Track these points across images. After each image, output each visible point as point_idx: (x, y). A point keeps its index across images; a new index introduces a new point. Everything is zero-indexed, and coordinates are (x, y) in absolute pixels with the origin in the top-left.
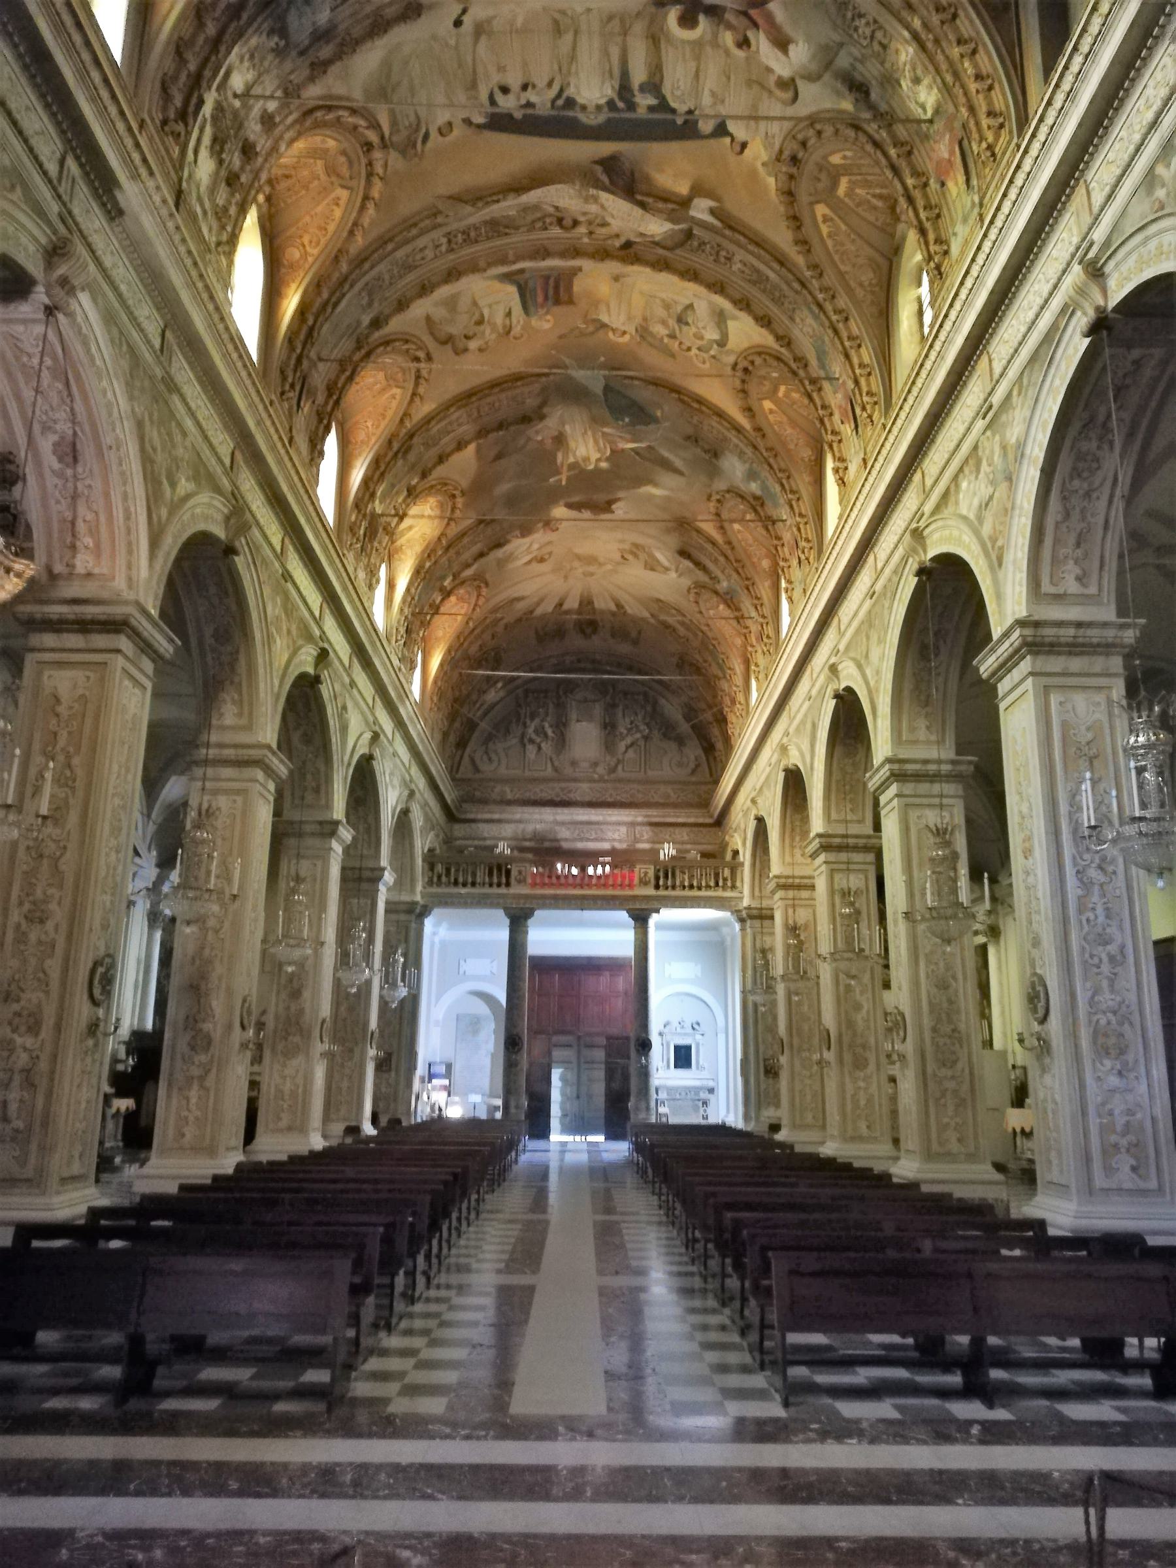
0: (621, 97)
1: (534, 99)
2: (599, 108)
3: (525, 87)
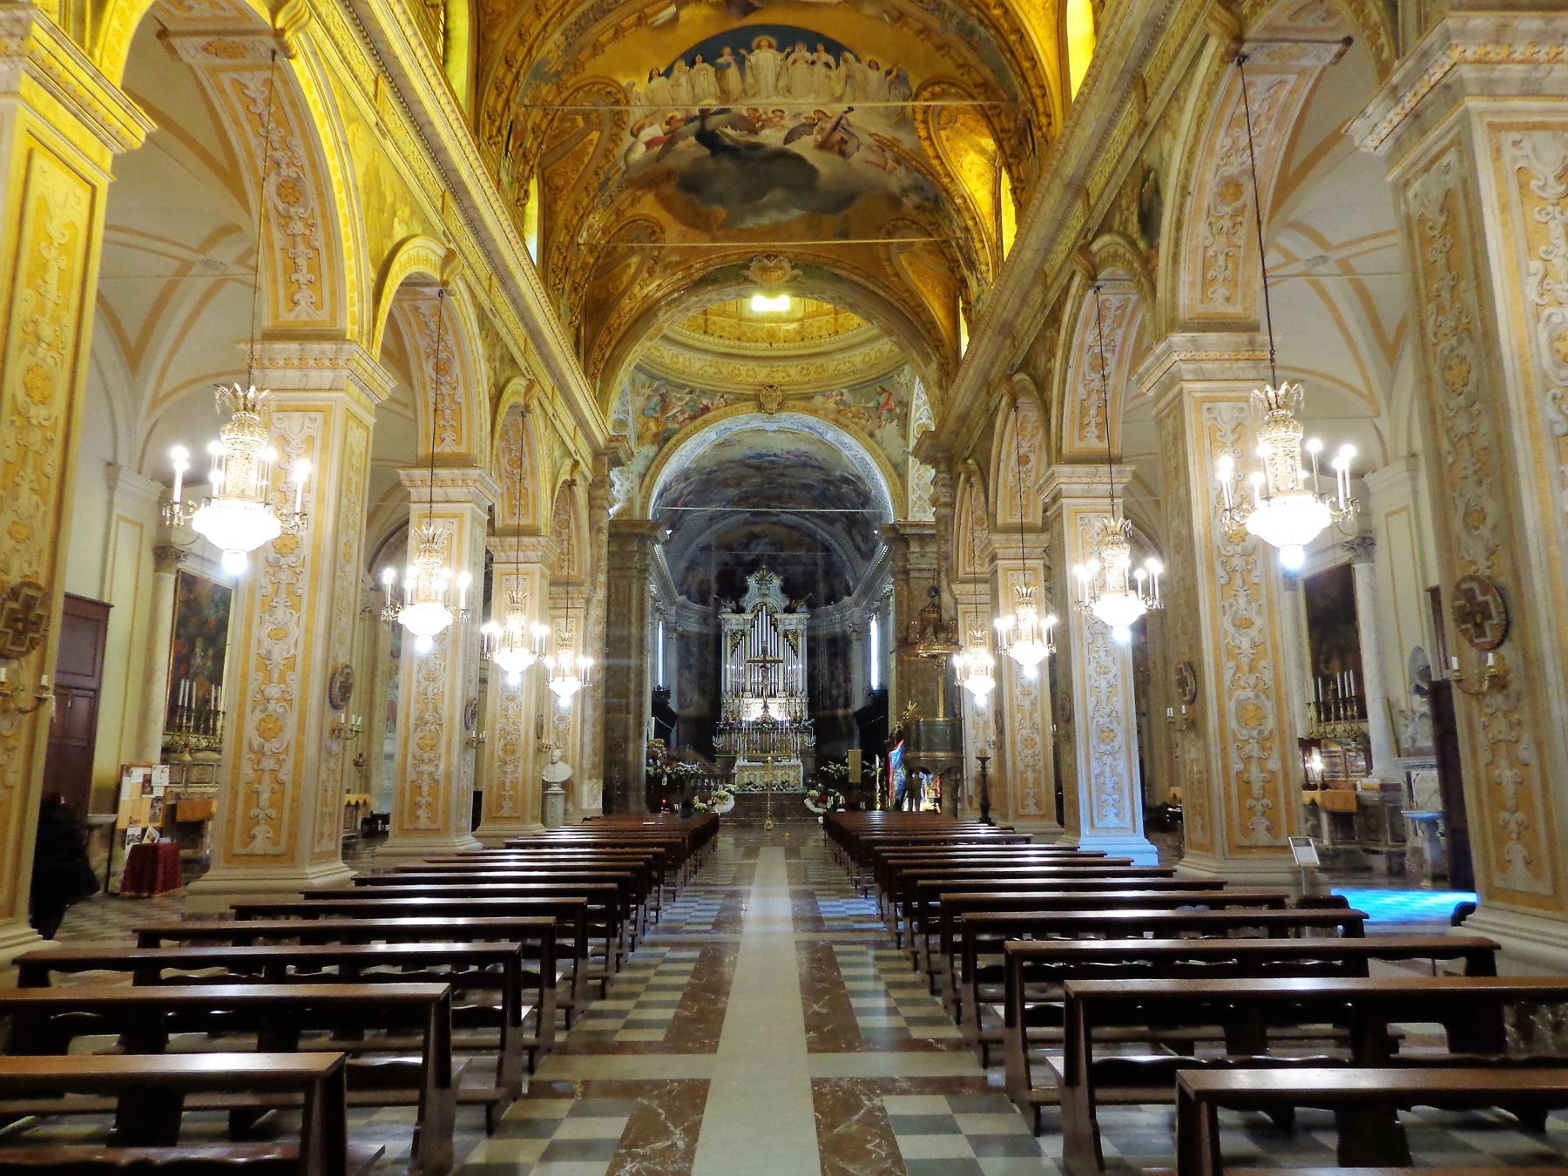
1: (808, 55)
2: (759, 47)
3: (813, 63)
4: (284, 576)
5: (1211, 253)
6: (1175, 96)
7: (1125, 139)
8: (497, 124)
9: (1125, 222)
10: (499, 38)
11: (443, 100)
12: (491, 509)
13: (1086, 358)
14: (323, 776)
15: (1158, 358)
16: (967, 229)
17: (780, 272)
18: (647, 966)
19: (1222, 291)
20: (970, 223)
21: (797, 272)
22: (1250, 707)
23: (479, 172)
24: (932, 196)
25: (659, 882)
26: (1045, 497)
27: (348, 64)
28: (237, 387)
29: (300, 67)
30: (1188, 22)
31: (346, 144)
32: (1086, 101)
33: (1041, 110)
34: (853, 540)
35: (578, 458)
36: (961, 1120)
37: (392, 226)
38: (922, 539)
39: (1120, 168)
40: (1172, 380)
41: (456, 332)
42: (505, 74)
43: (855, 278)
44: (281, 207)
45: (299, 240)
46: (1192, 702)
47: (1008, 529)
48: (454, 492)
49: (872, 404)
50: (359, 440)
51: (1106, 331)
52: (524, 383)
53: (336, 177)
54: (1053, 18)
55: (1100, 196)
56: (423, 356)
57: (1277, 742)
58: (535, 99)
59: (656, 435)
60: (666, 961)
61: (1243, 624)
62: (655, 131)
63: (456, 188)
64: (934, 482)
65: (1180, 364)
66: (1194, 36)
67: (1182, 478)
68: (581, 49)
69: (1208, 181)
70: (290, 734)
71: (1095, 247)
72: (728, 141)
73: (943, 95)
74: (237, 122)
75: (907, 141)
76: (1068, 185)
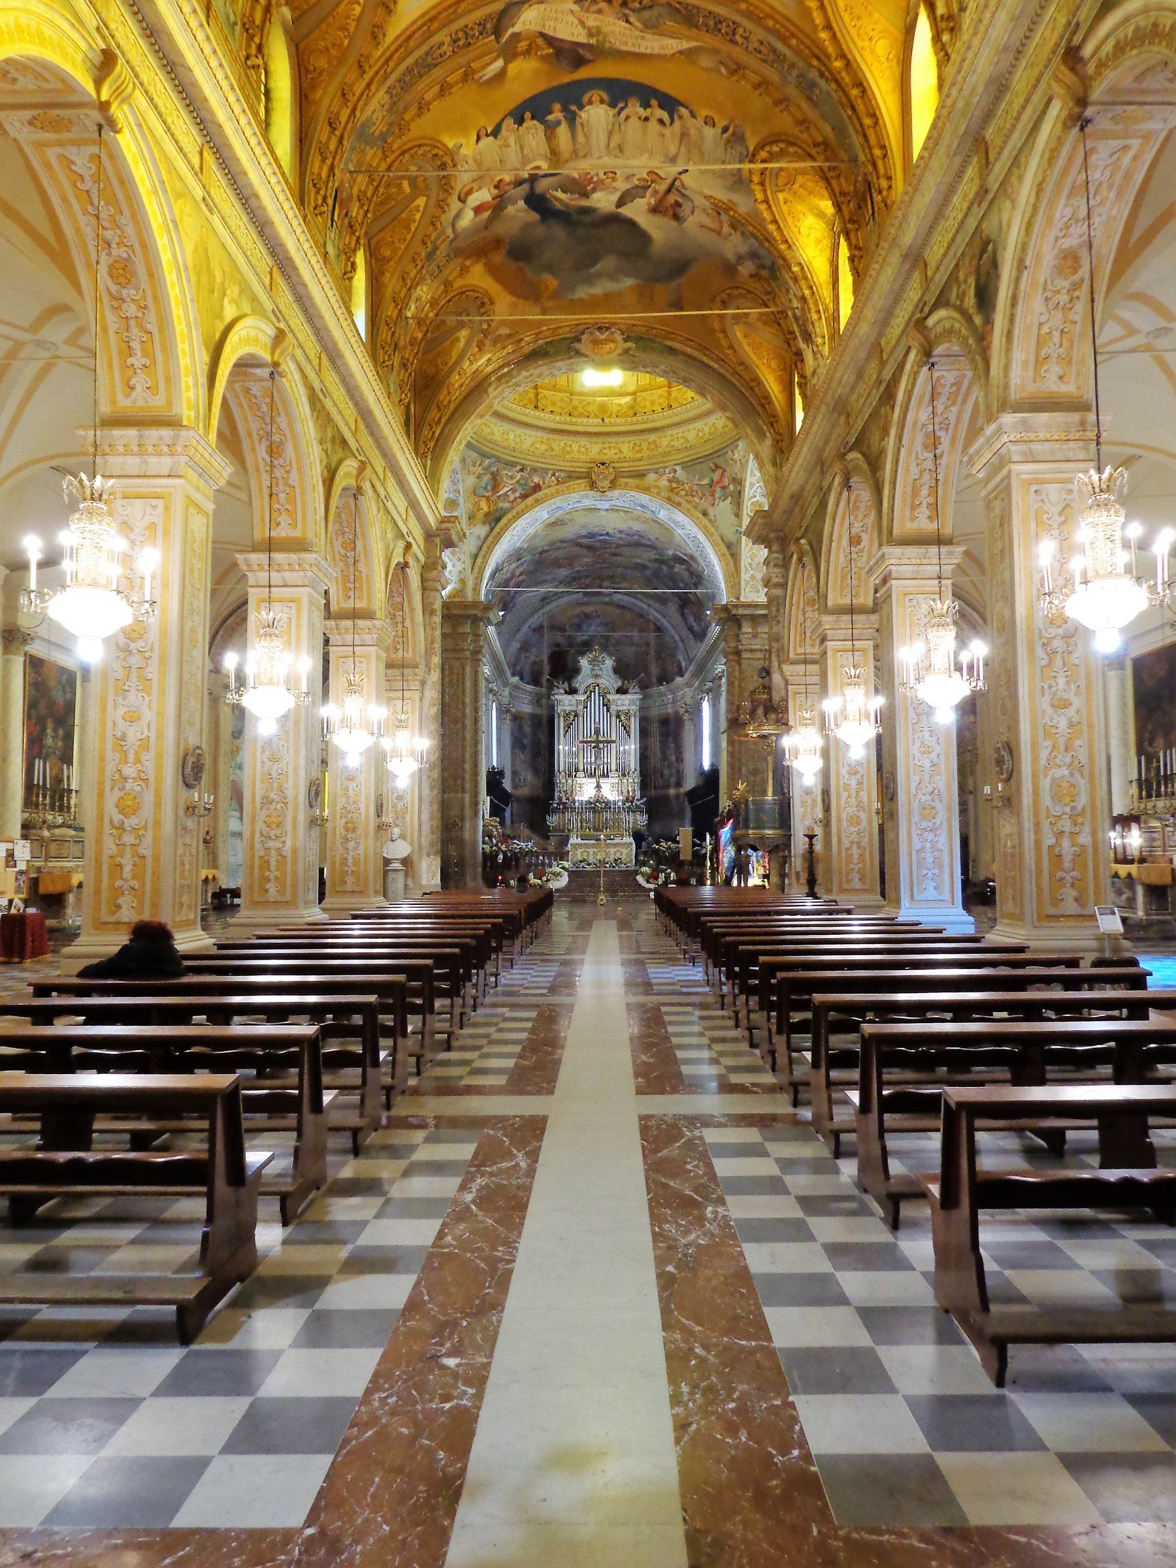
0: (574, 113)
1: (641, 110)
2: (590, 103)
3: (646, 119)
4: (135, 661)
5: (1045, 329)
6: (1016, 162)
7: (965, 206)
8: (322, 192)
9: (962, 296)
10: (321, 99)
11: (268, 171)
12: (326, 592)
13: (919, 438)
14: (180, 852)
15: (988, 440)
16: (803, 299)
17: (612, 345)
18: (489, 1025)
19: (1055, 369)
20: (807, 292)
21: (629, 344)
22: (1065, 784)
23: (306, 246)
24: (768, 262)
25: (498, 949)
26: (874, 580)
27: (172, 135)
28: (83, 476)
29: (126, 142)
30: (1032, 82)
31: (174, 222)
32: (926, 167)
33: (882, 172)
34: (685, 619)
35: (410, 539)
36: (770, 1147)
37: (222, 307)
38: (754, 619)
39: (959, 239)
40: (1002, 462)
41: (287, 415)
42: (329, 138)
43: (689, 350)
44: (114, 288)
45: (133, 323)
46: (1008, 780)
47: (840, 611)
48: (290, 577)
49: (705, 482)
50: (200, 527)
51: (940, 409)
52: (356, 464)
53: (165, 257)
54: (897, 71)
55: (938, 268)
56: (256, 440)
57: (1088, 817)
58: (359, 164)
59: (487, 515)
60: (506, 1020)
61: (1061, 705)
62: (483, 195)
63: (283, 264)
64: (767, 562)
65: (1009, 445)
66: (1038, 98)
67: (1007, 560)
68: (406, 109)
69: (1046, 254)
70: (147, 811)
71: (930, 322)
72: (558, 205)
73: (782, 154)
74: (65, 200)
75: (743, 205)
76: (905, 257)
